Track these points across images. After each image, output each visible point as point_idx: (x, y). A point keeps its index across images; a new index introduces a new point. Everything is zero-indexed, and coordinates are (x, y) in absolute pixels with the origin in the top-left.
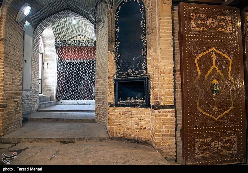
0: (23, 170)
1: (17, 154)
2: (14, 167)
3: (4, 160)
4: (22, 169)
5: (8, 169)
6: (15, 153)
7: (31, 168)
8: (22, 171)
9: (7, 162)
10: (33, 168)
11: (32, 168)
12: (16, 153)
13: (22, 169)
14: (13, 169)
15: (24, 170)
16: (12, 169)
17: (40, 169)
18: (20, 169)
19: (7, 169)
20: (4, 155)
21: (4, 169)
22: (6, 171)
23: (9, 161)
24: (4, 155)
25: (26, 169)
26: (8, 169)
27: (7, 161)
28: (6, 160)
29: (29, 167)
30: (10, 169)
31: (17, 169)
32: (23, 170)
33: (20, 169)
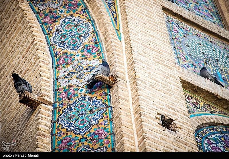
0: (21, 156)
2: (13, 153)
3: (4, 147)
4: (21, 156)
5: (8, 156)
6: (13, 141)
7: (28, 154)
8: (20, 158)
10: (30, 154)
11: (29, 155)
13: (21, 156)
14: (12, 156)
15: (22, 156)
16: (11, 156)
17: (37, 156)
18: (19, 156)
19: (7, 156)
20: (3, 142)
21: (4, 156)
22: (5, 157)
23: (8, 148)
24: (3, 142)
25: (24, 156)
26: (8, 156)
29: (27, 153)
30: (9, 156)
31: (16, 155)
32: (21, 156)
33: (19, 156)
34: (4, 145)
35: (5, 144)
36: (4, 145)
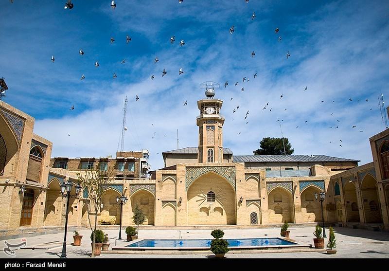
0: (36, 266)
1: (26, 242)
3: (7, 251)
4: (35, 265)
5: (13, 265)
6: (23, 240)
7: (48, 263)
8: (34, 268)
9: (10, 254)
10: (51, 263)
11: (50, 263)
12: (25, 240)
13: (35, 265)
14: (21, 265)
15: (38, 266)
16: (18, 265)
17: (63, 265)
18: (32, 265)
19: (11, 265)
20: (6, 242)
21: (7, 265)
22: (9, 268)
23: (14, 253)
24: (6, 242)
25: (40, 265)
26: (13, 265)
27: (12, 253)
28: (10, 251)
29: (46, 261)
30: (16, 265)
31: (27, 265)
32: (36, 266)
33: (32, 265)
34: (7, 247)
35: (9, 245)
36: (7, 247)
